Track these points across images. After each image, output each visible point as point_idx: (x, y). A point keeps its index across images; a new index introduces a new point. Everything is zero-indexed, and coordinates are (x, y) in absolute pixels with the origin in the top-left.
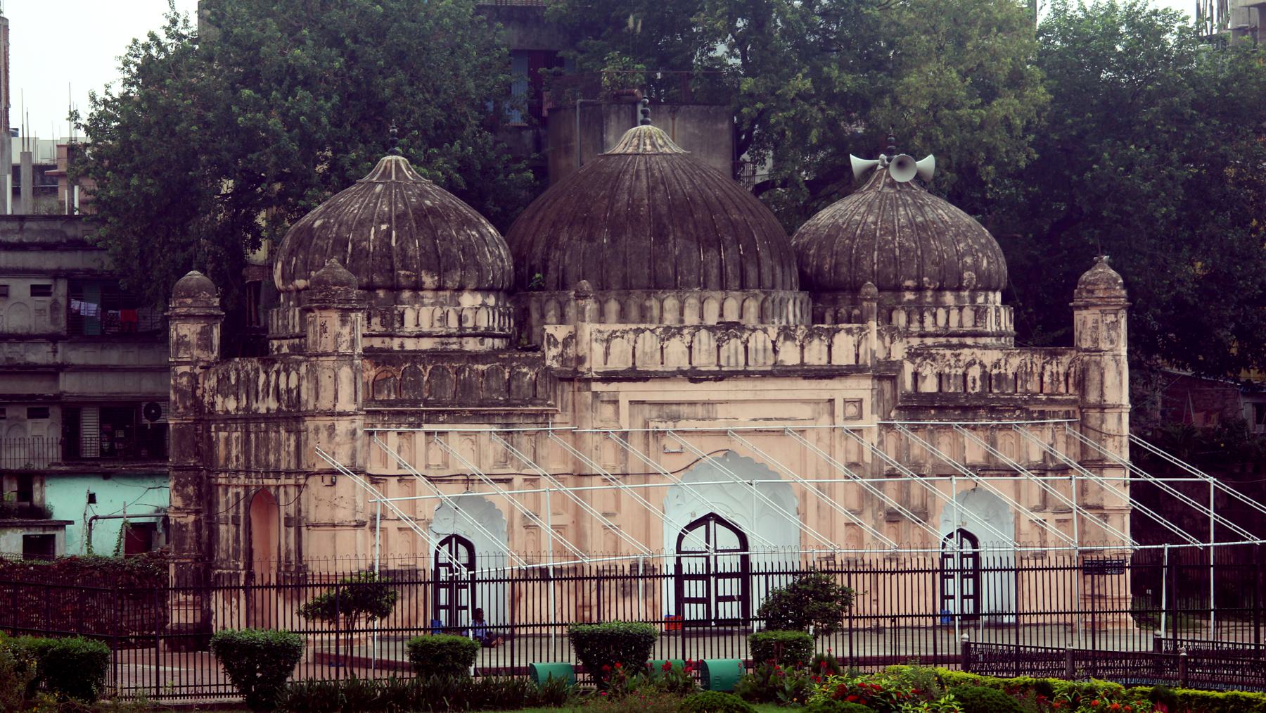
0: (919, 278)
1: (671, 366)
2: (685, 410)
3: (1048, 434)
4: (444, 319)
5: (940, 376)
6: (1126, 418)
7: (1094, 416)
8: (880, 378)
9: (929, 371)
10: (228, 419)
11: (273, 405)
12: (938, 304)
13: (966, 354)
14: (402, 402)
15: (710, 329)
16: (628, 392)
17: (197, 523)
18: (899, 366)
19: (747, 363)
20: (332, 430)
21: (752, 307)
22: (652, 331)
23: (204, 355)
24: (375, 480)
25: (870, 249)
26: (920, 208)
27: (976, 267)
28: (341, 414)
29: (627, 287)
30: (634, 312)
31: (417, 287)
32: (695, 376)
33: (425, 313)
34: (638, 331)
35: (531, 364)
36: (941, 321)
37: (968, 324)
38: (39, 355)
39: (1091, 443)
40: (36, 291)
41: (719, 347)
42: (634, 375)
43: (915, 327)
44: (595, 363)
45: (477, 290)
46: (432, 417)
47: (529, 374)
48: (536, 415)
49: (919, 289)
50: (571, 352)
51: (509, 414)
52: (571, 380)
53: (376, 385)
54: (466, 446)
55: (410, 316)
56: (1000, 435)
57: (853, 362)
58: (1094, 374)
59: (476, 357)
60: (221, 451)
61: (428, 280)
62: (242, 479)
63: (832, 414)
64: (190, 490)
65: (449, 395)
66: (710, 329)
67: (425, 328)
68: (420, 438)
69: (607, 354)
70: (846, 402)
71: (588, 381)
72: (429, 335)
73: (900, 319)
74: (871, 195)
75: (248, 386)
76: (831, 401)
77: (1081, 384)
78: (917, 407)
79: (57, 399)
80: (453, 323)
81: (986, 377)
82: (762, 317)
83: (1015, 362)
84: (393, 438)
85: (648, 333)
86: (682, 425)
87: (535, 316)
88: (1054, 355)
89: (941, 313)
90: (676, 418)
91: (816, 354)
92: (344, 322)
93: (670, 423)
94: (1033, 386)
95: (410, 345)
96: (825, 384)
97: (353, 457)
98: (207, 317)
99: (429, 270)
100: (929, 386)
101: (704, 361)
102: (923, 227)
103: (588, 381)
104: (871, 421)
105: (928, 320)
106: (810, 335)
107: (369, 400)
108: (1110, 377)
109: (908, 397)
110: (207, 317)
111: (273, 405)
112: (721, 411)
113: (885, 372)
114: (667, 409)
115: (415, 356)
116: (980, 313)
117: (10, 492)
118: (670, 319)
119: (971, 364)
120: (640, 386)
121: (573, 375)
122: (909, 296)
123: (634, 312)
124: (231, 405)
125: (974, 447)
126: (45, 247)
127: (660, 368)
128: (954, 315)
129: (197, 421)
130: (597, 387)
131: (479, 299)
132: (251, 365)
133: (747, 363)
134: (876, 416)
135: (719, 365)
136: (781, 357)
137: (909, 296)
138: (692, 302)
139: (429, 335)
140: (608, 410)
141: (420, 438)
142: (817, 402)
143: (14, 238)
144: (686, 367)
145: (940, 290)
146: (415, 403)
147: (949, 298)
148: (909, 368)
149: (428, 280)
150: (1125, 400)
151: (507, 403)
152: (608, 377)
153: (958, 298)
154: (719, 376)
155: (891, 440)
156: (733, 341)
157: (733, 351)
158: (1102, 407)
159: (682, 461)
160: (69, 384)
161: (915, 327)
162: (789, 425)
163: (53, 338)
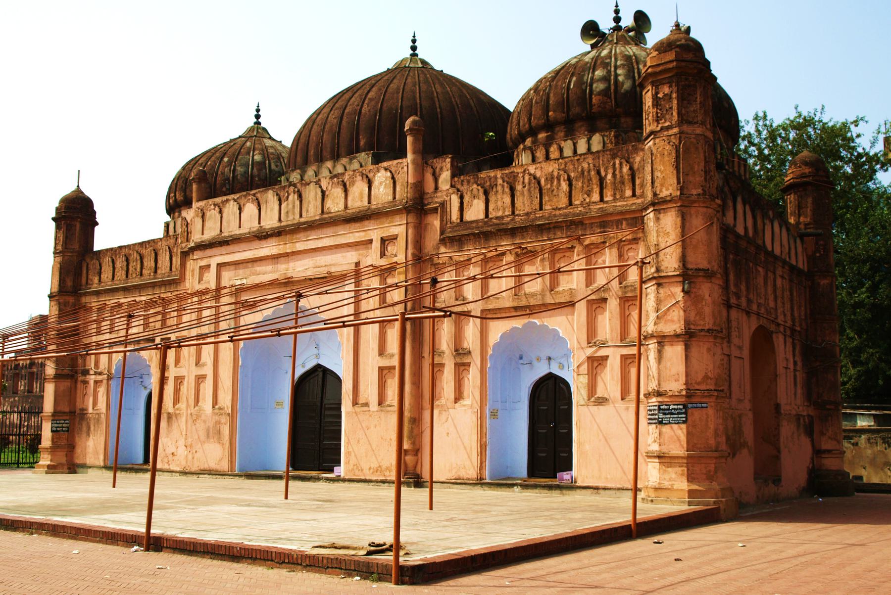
1: (245, 230)
19: (301, 216)
22: (235, 200)
32: (262, 236)
41: (280, 205)
57: (390, 198)
70: (383, 241)
71: (192, 250)
76: (371, 241)
85: (232, 202)
100: (475, 211)
120: (224, 249)
127: (238, 232)
133: (301, 216)
135: (280, 220)
136: (329, 204)
144: (255, 225)
156: (291, 198)
157: (291, 206)
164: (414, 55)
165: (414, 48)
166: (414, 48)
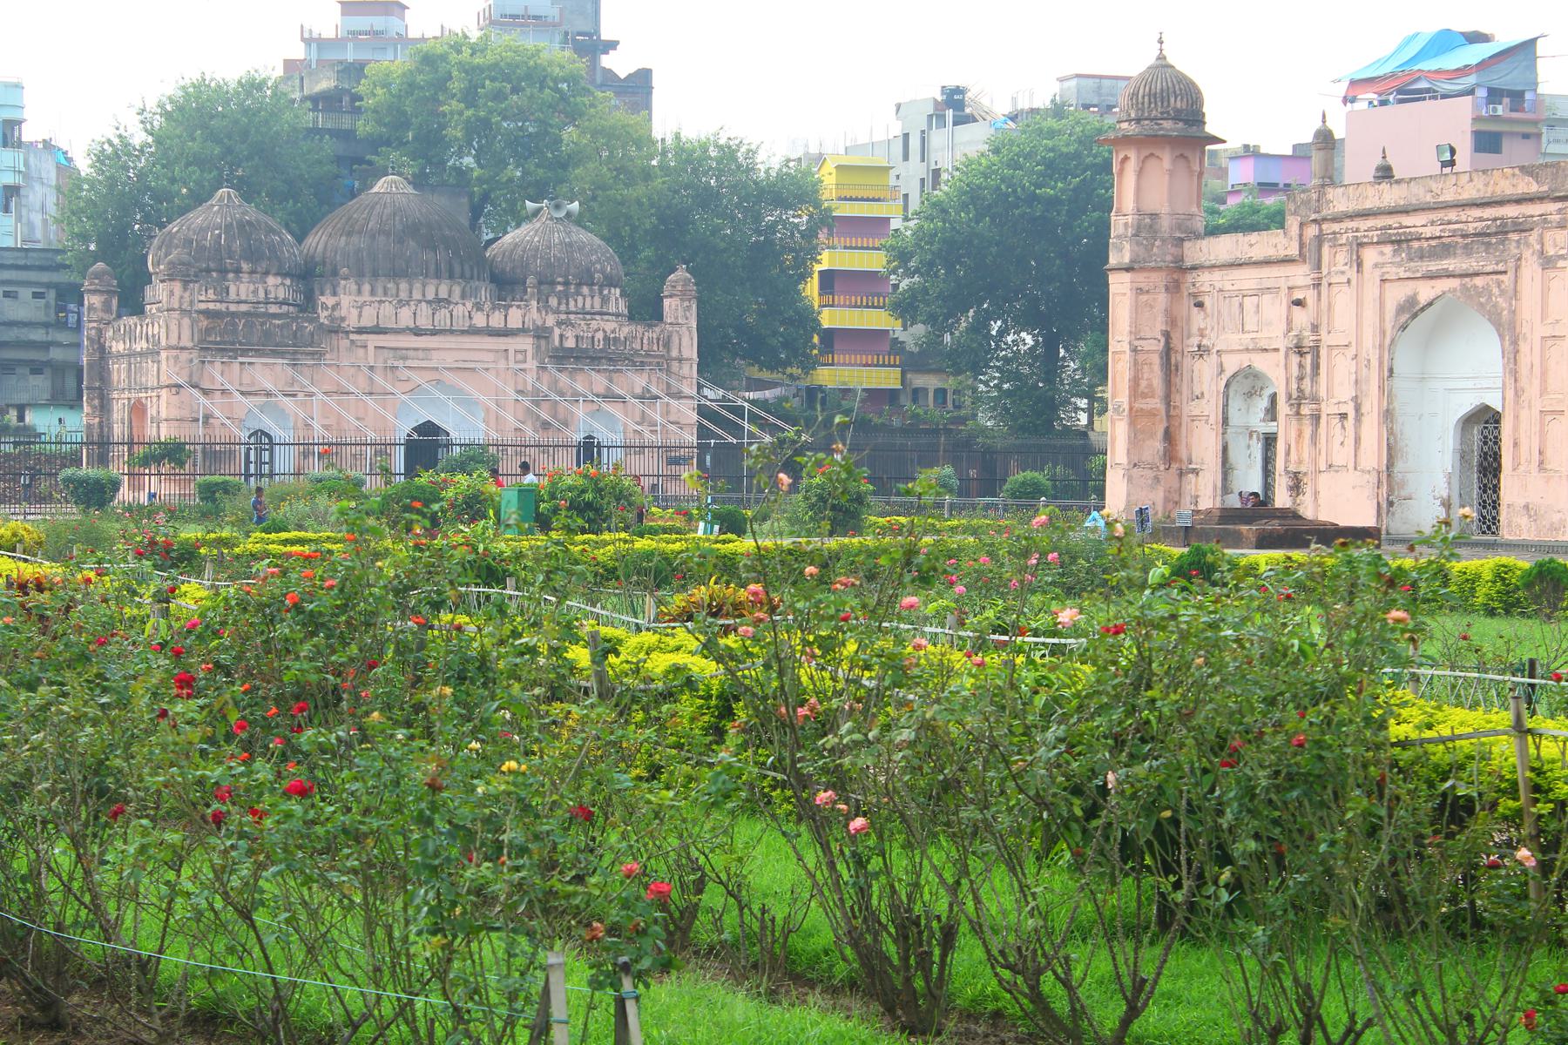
0: (566, 277)
1: (402, 325)
2: (411, 353)
3: (645, 375)
4: (255, 292)
5: (577, 337)
6: (695, 367)
7: (675, 365)
8: (538, 337)
9: (570, 333)
10: (120, 356)
11: (145, 345)
12: (578, 293)
13: (594, 325)
14: (224, 343)
15: (429, 302)
16: (373, 340)
17: (101, 423)
18: (550, 330)
20: (177, 358)
21: (457, 290)
23: (106, 316)
24: (206, 392)
25: (535, 257)
26: (569, 234)
27: (602, 271)
28: (182, 348)
29: (375, 274)
30: (380, 291)
31: (238, 271)
32: (418, 332)
33: (243, 288)
34: (381, 302)
35: (311, 321)
36: (580, 305)
37: (597, 307)
38: (38, 335)
39: (673, 382)
40: (36, 295)
42: (377, 330)
43: (563, 308)
44: (352, 322)
45: (277, 274)
46: (244, 353)
47: (310, 328)
49: (566, 284)
50: (336, 314)
51: (295, 353)
52: (336, 332)
53: (208, 331)
54: (266, 373)
55: (233, 289)
56: (615, 376)
58: (675, 339)
59: (275, 316)
60: (115, 377)
61: (245, 266)
62: (126, 395)
63: (507, 359)
64: (96, 402)
65: (255, 339)
66: (429, 302)
67: (243, 297)
68: (236, 367)
69: (360, 316)
72: (245, 302)
73: (553, 302)
74: (538, 225)
75: (130, 335)
77: (667, 345)
78: (562, 357)
79: (49, 363)
80: (262, 295)
81: (606, 338)
82: (463, 296)
83: (626, 330)
84: (218, 365)
87: (317, 292)
88: (650, 326)
89: (580, 299)
90: (405, 358)
91: (497, 320)
92: (185, 289)
93: (400, 364)
95: (233, 308)
96: (502, 339)
97: (191, 376)
98: (108, 292)
99: (248, 259)
100: (570, 343)
101: (424, 322)
102: (570, 245)
104: (532, 364)
105: (572, 303)
106: (493, 309)
107: (201, 341)
108: (686, 340)
109: (556, 349)
110: (108, 292)
111: (145, 345)
113: (541, 334)
115: (234, 315)
116: (605, 300)
117: (12, 416)
118: (403, 295)
119: (597, 330)
120: (381, 337)
121: (336, 329)
122: (560, 288)
123: (380, 291)
124: (121, 347)
125: (600, 382)
126: (42, 268)
128: (588, 300)
129: (102, 358)
130: (353, 337)
131: (279, 280)
132: (133, 320)
137: (560, 288)
138: (417, 285)
139: (245, 302)
140: (361, 352)
141: (236, 367)
143: (22, 262)
144: (412, 325)
145: (579, 285)
146: (233, 343)
147: (585, 290)
148: (557, 331)
149: (245, 266)
150: (695, 356)
151: (294, 345)
152: (360, 331)
153: (591, 290)
155: (545, 377)
158: (680, 360)
159: (409, 386)
160: (56, 354)
161: (563, 308)
162: (478, 365)
163: (46, 325)
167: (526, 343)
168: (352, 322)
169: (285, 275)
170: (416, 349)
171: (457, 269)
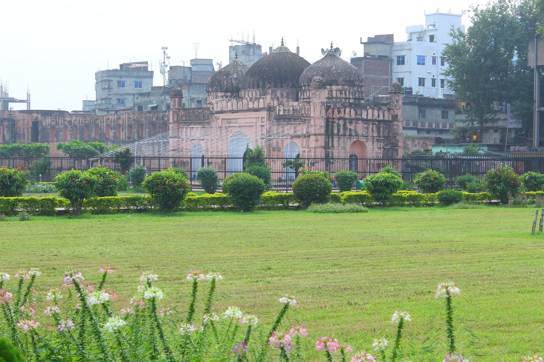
2: (232, 121)
5: (284, 110)
9: (282, 109)
16: (221, 116)
32: (233, 112)
36: (308, 95)
42: (222, 112)
43: (302, 97)
45: (221, 91)
46: (191, 124)
48: (208, 123)
49: (305, 86)
51: (204, 123)
70: (262, 118)
81: (293, 110)
86: (231, 125)
89: (308, 92)
90: (230, 123)
94: (303, 112)
96: (258, 113)
100: (282, 113)
101: (235, 108)
103: (214, 114)
109: (277, 116)
112: (239, 121)
113: (270, 109)
114: (229, 121)
130: (216, 115)
131: (223, 94)
134: (268, 122)
142: (257, 118)
148: (278, 108)
152: (217, 113)
154: (237, 112)
164: (283, 45)
165: (282, 42)
166: (282, 42)
167: (264, 114)
168: (215, 110)
169: (226, 91)
170: (233, 119)
171: (261, 84)
